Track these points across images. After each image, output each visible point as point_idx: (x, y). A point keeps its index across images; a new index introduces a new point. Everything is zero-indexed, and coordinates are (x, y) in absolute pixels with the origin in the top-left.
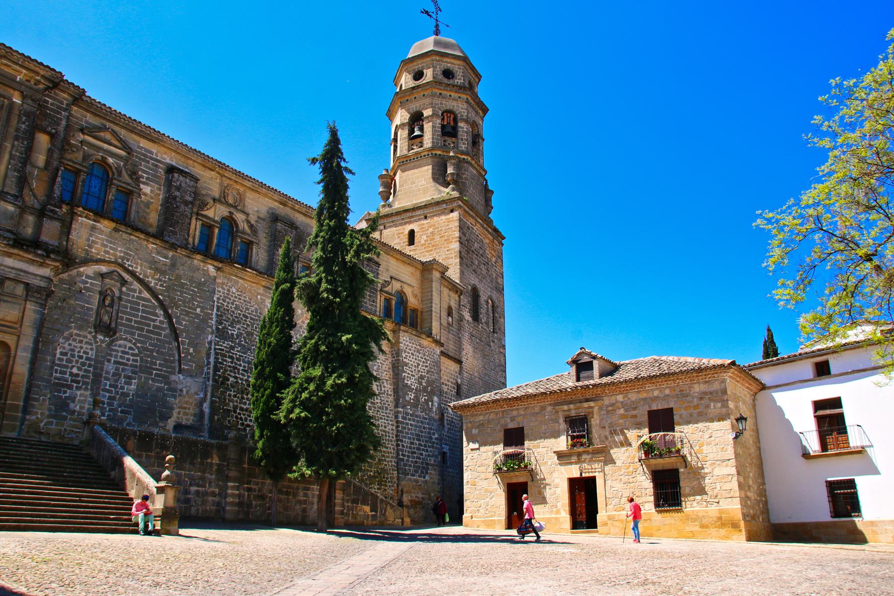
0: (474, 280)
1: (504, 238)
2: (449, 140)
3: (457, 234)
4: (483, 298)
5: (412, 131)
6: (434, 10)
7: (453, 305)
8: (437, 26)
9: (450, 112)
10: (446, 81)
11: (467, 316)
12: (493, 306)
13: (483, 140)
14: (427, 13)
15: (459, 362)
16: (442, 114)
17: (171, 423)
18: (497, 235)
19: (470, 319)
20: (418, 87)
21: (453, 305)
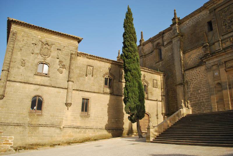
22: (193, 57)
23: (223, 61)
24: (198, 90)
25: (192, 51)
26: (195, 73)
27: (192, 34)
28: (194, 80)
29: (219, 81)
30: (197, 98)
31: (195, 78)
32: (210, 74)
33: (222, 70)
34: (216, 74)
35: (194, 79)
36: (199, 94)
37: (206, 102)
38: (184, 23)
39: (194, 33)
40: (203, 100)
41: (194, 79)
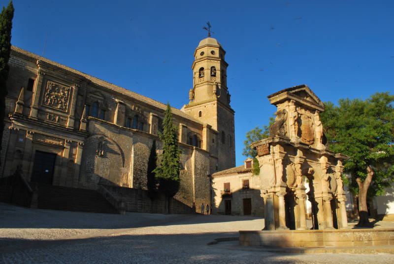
0: (223, 129)
1: (234, 112)
2: (214, 78)
3: (216, 113)
4: (226, 135)
5: (200, 75)
7: (214, 138)
8: (209, 34)
9: (214, 67)
10: (212, 56)
11: (219, 141)
12: (231, 138)
15: (217, 158)
18: (232, 112)
19: (221, 143)
20: (202, 58)
21: (214, 138)
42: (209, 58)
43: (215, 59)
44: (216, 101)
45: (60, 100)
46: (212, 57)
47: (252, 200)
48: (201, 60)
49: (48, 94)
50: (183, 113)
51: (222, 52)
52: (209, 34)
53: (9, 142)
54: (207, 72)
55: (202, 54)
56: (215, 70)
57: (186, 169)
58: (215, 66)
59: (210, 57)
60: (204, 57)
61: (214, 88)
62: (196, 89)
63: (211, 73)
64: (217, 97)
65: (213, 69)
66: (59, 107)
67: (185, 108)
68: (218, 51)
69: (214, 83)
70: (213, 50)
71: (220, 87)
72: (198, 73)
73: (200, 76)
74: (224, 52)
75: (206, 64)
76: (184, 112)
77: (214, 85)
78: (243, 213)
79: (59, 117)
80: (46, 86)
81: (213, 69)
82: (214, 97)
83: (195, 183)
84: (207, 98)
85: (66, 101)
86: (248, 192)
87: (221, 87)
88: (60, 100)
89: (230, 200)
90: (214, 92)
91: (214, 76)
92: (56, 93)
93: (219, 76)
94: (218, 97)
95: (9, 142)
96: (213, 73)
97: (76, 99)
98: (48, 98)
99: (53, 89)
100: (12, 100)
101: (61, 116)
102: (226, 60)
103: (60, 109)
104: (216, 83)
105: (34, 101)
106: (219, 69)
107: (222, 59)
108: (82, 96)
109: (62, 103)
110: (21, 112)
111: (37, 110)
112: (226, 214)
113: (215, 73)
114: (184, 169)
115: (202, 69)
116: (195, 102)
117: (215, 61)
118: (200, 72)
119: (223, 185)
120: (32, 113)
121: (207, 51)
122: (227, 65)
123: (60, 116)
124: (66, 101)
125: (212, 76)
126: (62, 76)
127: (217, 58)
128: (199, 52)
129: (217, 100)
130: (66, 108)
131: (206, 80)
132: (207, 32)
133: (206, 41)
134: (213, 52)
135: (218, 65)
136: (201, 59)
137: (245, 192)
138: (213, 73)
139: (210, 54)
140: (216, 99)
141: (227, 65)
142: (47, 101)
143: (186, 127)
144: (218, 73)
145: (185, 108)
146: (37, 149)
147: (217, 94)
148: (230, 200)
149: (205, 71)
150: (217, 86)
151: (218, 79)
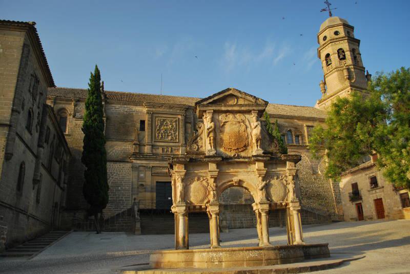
2: (343, 61)
6: (327, 6)
9: (341, 49)
10: (336, 37)
13: (360, 55)
14: (324, 10)
16: (338, 51)
17: (243, 199)
22: (116, 149)
23: (151, 166)
24: (119, 186)
25: (117, 142)
26: (118, 167)
27: (120, 123)
28: (115, 174)
29: (143, 183)
30: (116, 195)
31: (117, 173)
32: (136, 174)
33: (149, 173)
34: (142, 175)
35: (115, 173)
36: (119, 190)
37: (126, 200)
38: (113, 105)
39: (124, 123)
40: (122, 197)
41: (115, 173)
42: (333, 41)
43: (342, 39)
44: (350, 88)
45: (170, 132)
46: (337, 39)
47: (383, 200)
48: (324, 46)
49: (158, 130)
50: (319, 111)
51: (348, 28)
52: (330, 13)
53: (132, 178)
54: (334, 58)
55: (325, 38)
56: (343, 52)
57: (320, 173)
58: (342, 47)
59: (333, 39)
60: (339, 38)
61: (346, 73)
62: (326, 79)
63: (339, 57)
64: (351, 83)
65: (340, 52)
66: (170, 138)
67: (319, 104)
68: (342, 29)
69: (344, 67)
70: (337, 30)
71: (353, 70)
72: (325, 62)
73: (328, 65)
74: (352, 28)
75: (331, 49)
76: (318, 108)
77: (344, 69)
78: (375, 217)
79: (172, 148)
80: (155, 123)
81: (341, 51)
82: (347, 83)
83: (333, 187)
84: (339, 87)
85: (175, 131)
86: (377, 191)
87: (354, 68)
88: (170, 132)
89: (361, 203)
90: (345, 77)
91: (344, 58)
92: (165, 127)
93: (350, 57)
94: (353, 81)
95: (132, 178)
96: (341, 57)
97: (184, 128)
98: (159, 133)
99: (162, 125)
100: (129, 143)
101: (173, 146)
102: (356, 37)
103: (171, 140)
104: (347, 66)
105: (147, 138)
106: (348, 49)
107: (348, 37)
108: (190, 123)
109: (171, 135)
110: (137, 151)
111: (150, 146)
112: (360, 220)
113: (344, 56)
114: (318, 173)
115: (328, 56)
116: (328, 93)
117: (342, 42)
118: (326, 60)
119: (351, 187)
120: (147, 149)
121: (329, 34)
122: (358, 42)
123: (171, 146)
124: (175, 131)
125: (341, 59)
126: (168, 110)
127: (343, 38)
128: (321, 37)
129: (351, 86)
130: (176, 139)
131: (334, 67)
132: (327, 13)
133: (326, 23)
134: (336, 33)
135: (345, 45)
136: (323, 45)
137: (374, 191)
138: (341, 57)
139: (334, 35)
140: (349, 85)
141: (358, 42)
142: (158, 136)
143: (312, 127)
144: (348, 54)
145: (319, 104)
146: (157, 180)
147: (350, 78)
148: (361, 203)
149: (332, 57)
150: (348, 69)
151: (349, 61)
